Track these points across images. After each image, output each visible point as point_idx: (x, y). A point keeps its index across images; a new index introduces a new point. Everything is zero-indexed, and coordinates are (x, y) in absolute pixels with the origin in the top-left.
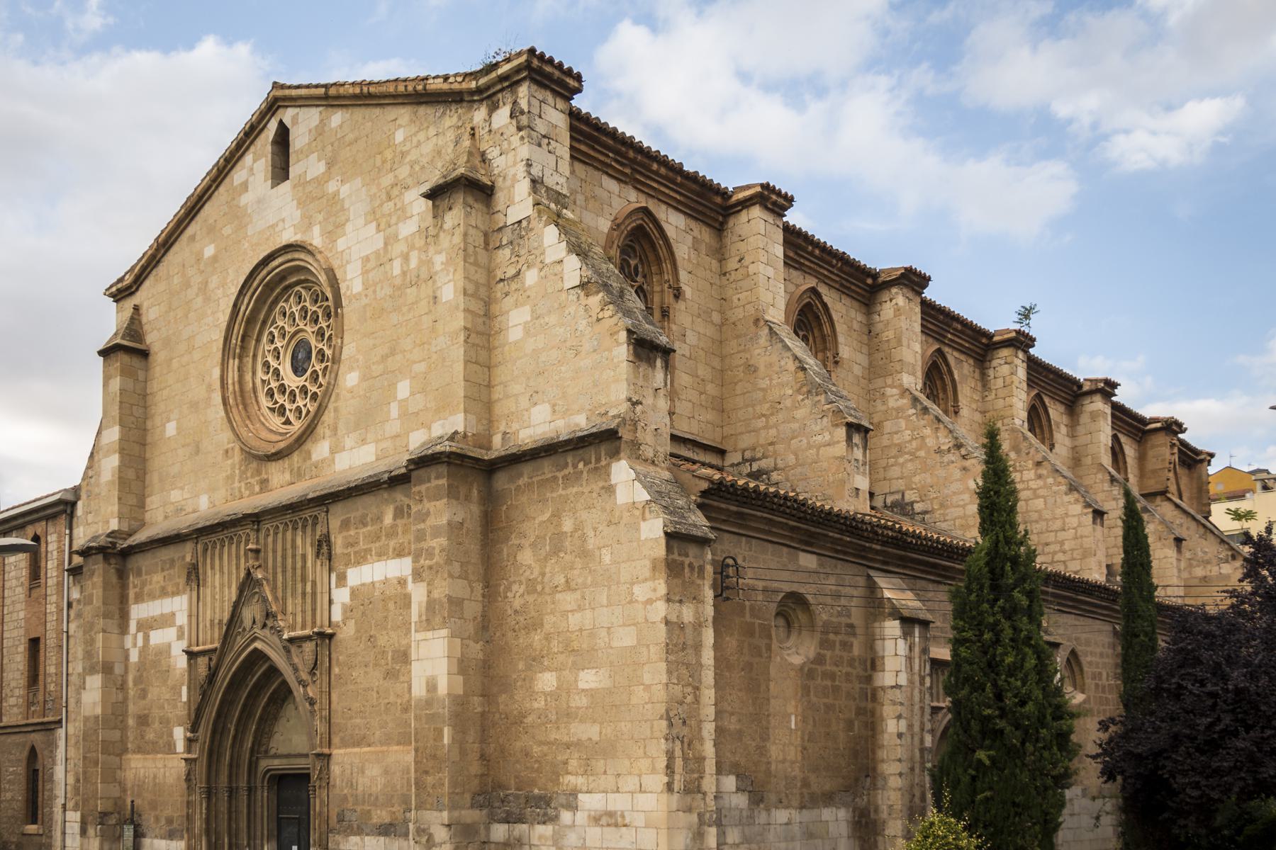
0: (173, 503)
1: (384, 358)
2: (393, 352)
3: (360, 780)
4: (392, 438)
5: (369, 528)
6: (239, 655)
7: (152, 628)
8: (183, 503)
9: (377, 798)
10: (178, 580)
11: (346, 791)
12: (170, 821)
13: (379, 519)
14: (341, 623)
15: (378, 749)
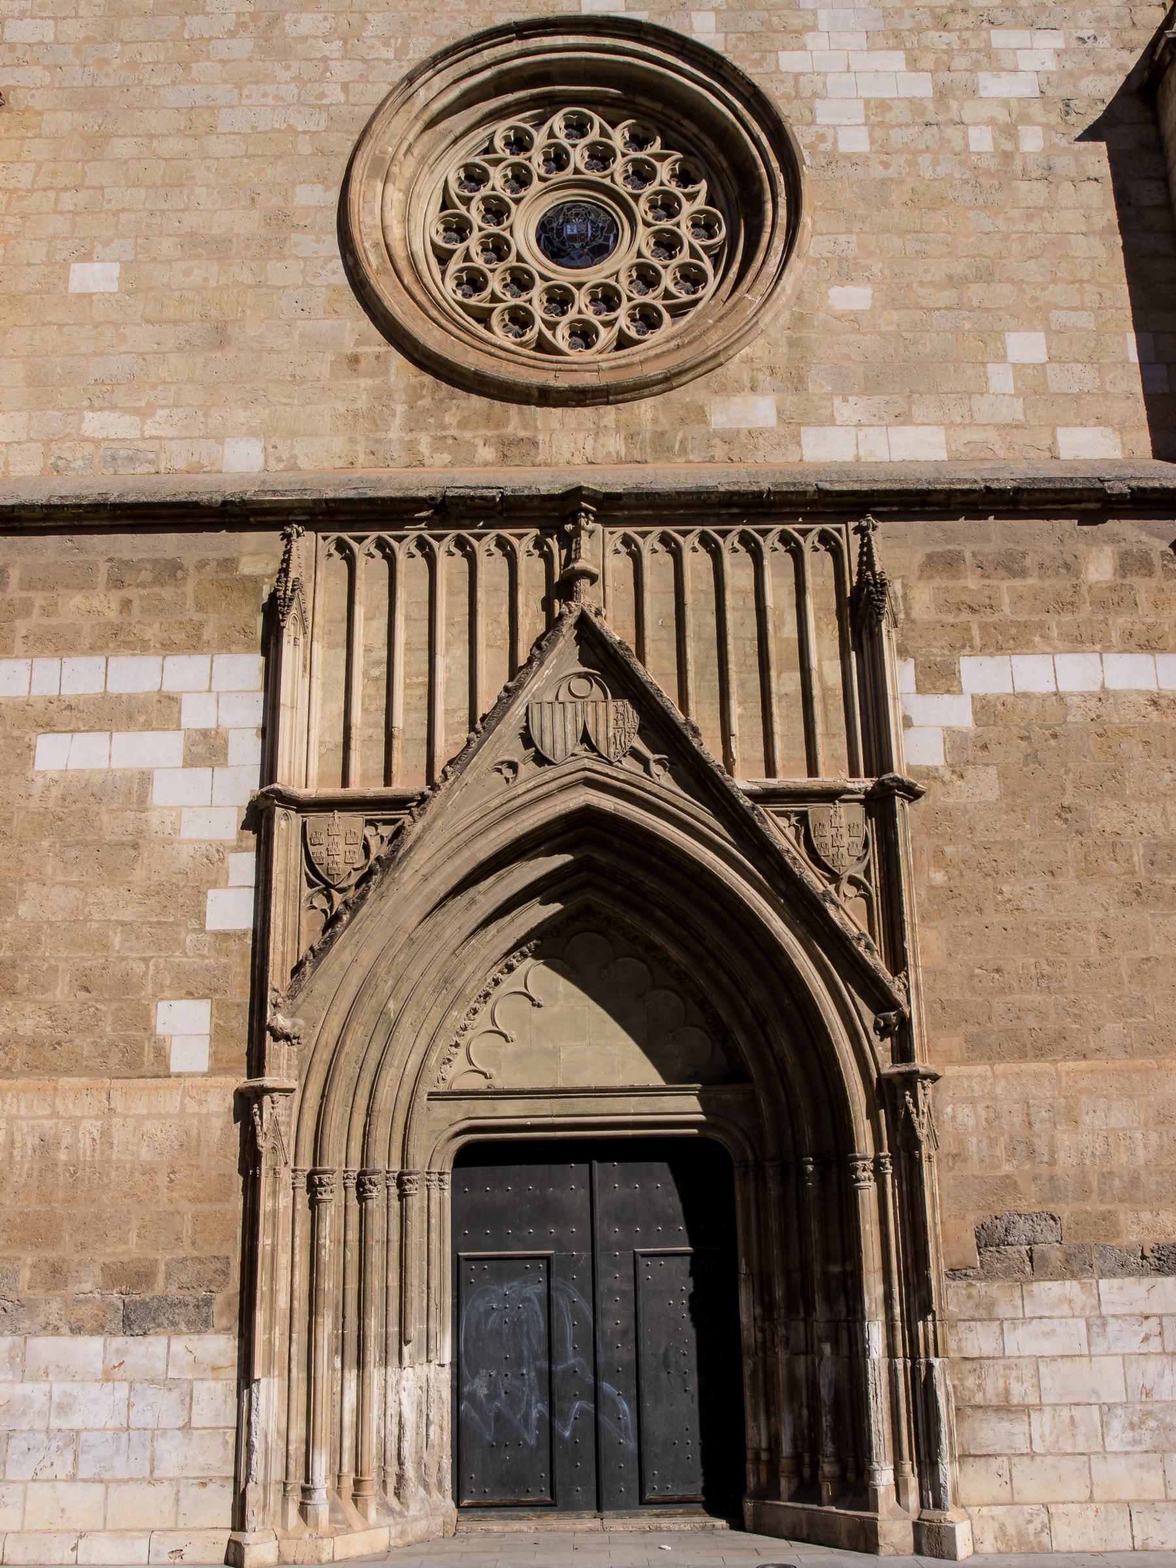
0: (96, 442)
1: (952, 281)
2: (986, 275)
3: (1064, 1139)
4: (1001, 427)
5: (1031, 581)
6: (506, 817)
7: (49, 727)
8: (141, 445)
9: (1135, 1182)
10: (197, 617)
11: (1007, 1168)
12: (114, 1276)
13: (1070, 567)
14: (947, 775)
15: (1117, 1064)
